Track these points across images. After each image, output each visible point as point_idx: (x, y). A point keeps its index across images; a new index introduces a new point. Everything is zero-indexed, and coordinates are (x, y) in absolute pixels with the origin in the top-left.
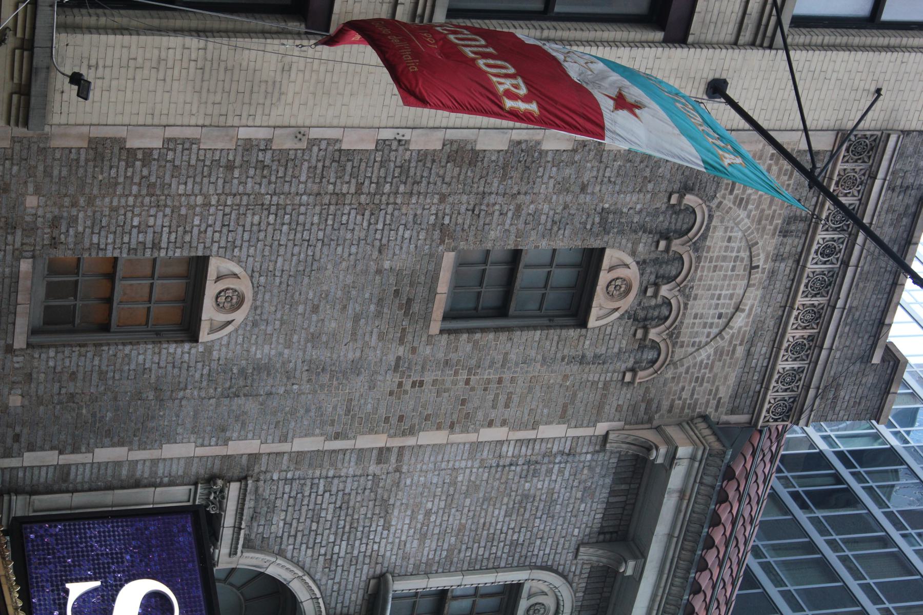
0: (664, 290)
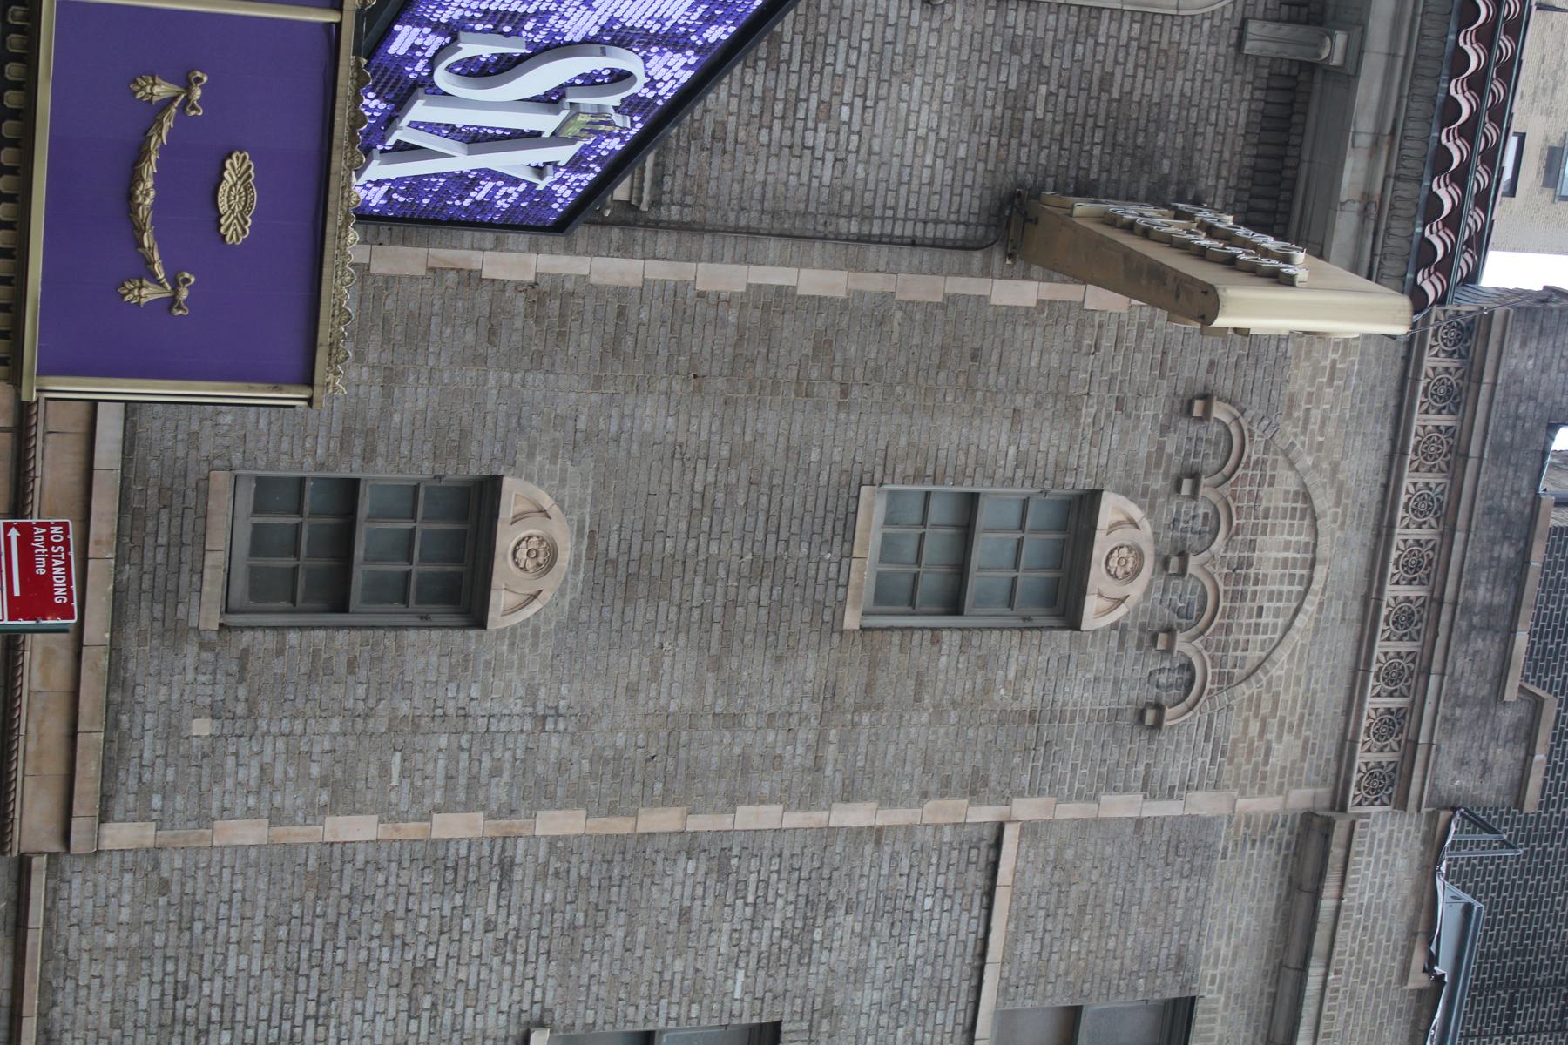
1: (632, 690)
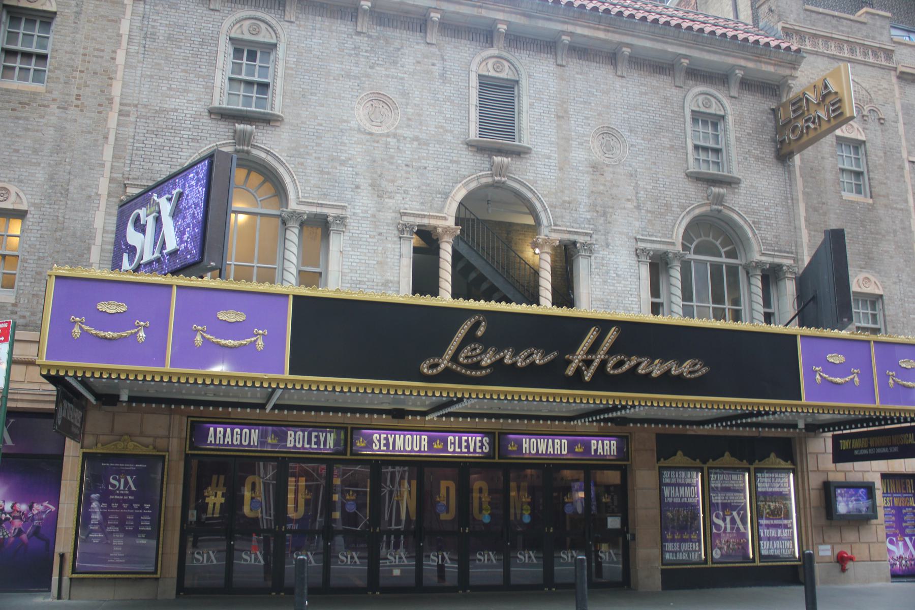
1: (892, 257)
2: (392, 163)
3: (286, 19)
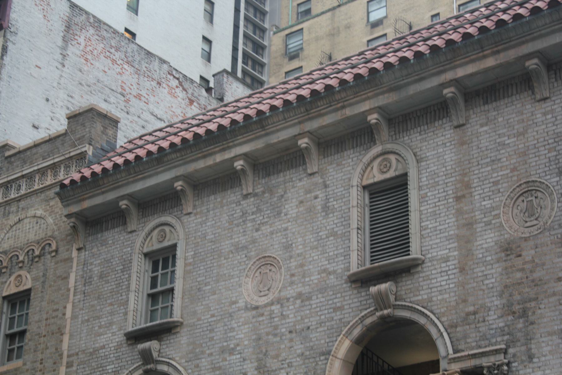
0: (21, 258)
2: (275, 335)
3: (184, 212)
